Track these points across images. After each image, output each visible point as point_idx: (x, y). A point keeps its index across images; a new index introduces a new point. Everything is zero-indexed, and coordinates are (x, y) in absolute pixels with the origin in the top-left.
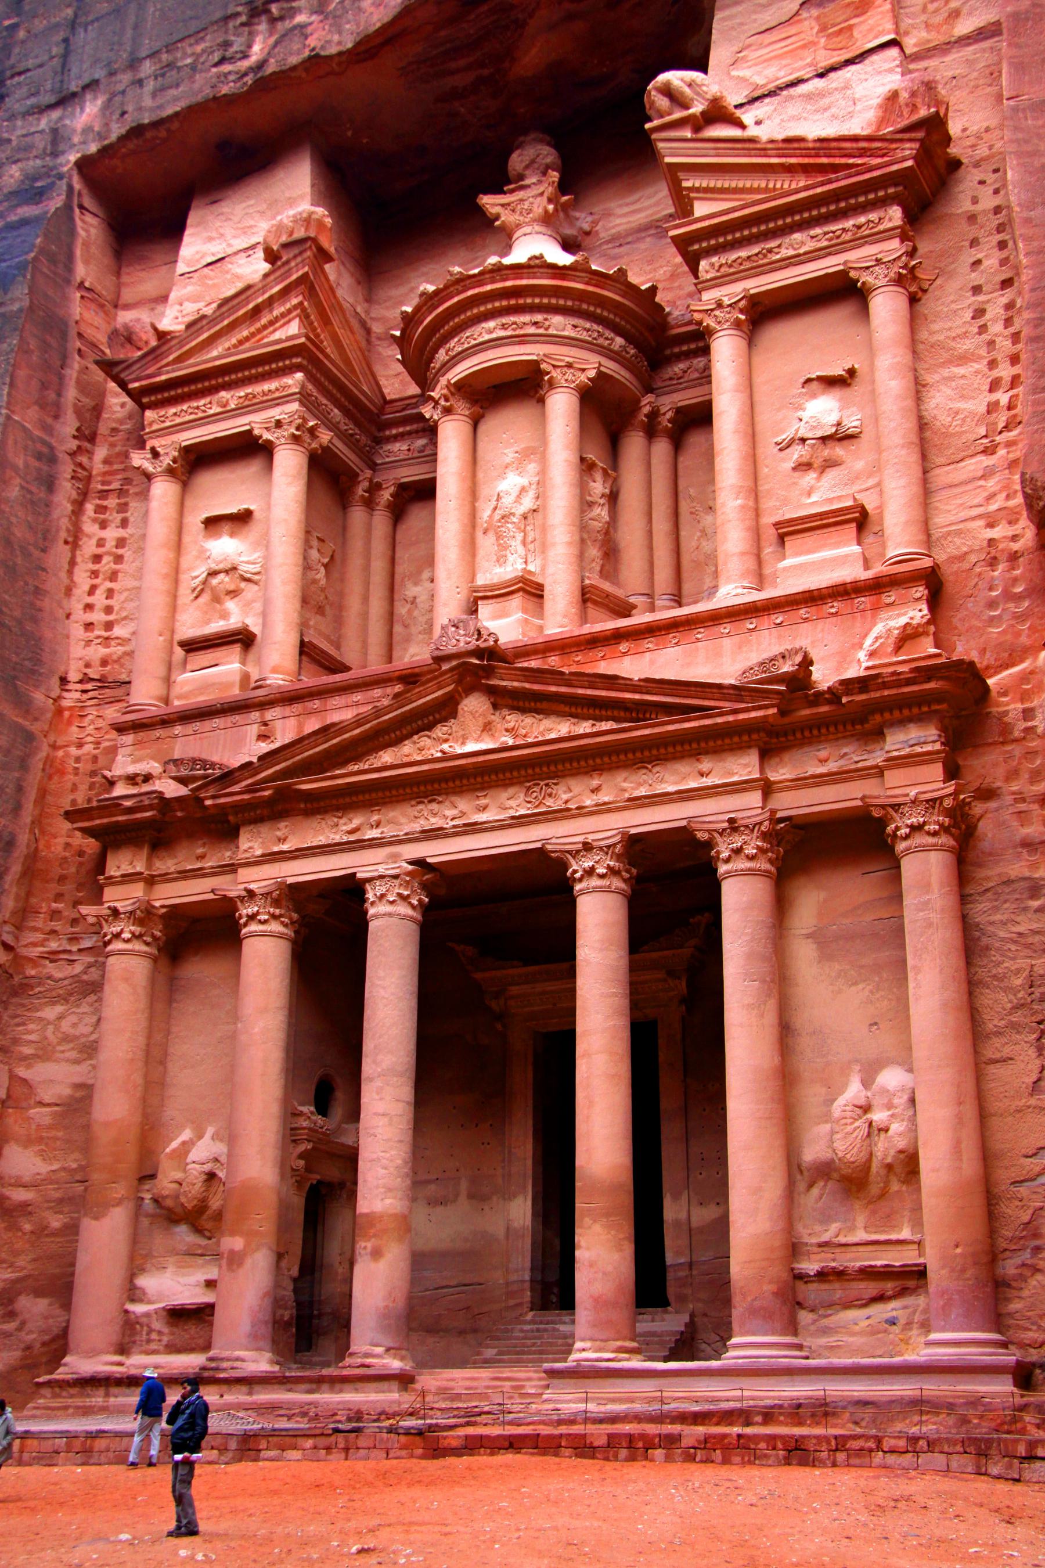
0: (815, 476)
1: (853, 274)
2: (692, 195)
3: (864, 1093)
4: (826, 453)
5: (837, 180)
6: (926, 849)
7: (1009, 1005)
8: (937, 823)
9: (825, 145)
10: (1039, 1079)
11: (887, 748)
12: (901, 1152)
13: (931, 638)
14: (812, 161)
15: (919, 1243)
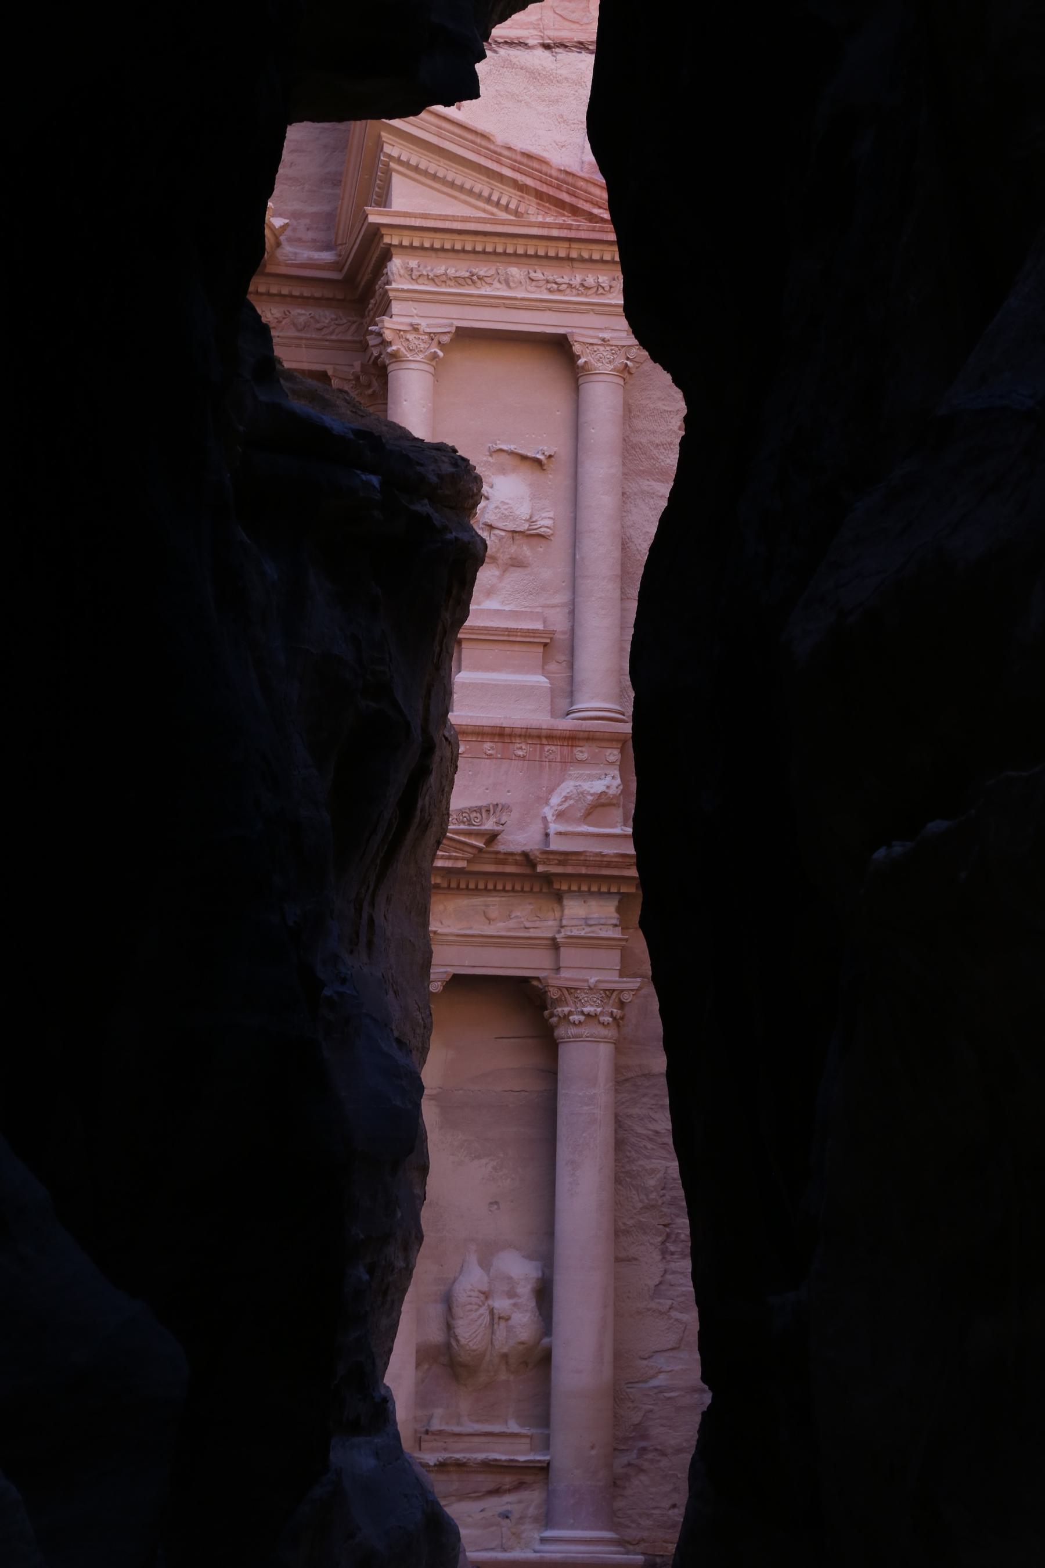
0: (497, 573)
1: (577, 348)
2: (392, 165)
3: (486, 1279)
4: (513, 549)
5: (578, 229)
6: (596, 1040)
7: (640, 1205)
8: (611, 1015)
9: (570, 179)
10: (661, 1283)
11: (564, 922)
12: (523, 1343)
13: (621, 810)
14: (552, 192)
15: (531, 1437)
